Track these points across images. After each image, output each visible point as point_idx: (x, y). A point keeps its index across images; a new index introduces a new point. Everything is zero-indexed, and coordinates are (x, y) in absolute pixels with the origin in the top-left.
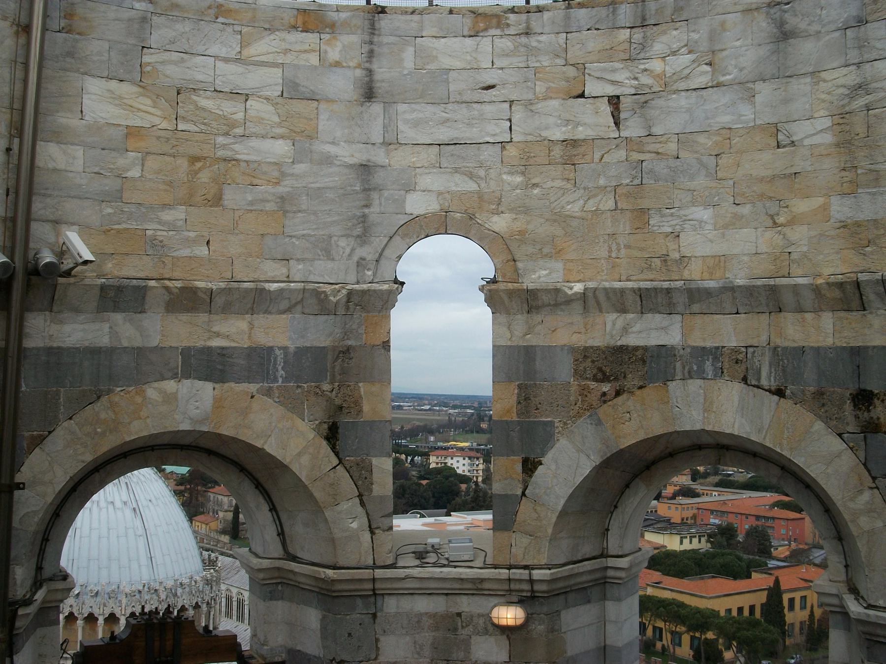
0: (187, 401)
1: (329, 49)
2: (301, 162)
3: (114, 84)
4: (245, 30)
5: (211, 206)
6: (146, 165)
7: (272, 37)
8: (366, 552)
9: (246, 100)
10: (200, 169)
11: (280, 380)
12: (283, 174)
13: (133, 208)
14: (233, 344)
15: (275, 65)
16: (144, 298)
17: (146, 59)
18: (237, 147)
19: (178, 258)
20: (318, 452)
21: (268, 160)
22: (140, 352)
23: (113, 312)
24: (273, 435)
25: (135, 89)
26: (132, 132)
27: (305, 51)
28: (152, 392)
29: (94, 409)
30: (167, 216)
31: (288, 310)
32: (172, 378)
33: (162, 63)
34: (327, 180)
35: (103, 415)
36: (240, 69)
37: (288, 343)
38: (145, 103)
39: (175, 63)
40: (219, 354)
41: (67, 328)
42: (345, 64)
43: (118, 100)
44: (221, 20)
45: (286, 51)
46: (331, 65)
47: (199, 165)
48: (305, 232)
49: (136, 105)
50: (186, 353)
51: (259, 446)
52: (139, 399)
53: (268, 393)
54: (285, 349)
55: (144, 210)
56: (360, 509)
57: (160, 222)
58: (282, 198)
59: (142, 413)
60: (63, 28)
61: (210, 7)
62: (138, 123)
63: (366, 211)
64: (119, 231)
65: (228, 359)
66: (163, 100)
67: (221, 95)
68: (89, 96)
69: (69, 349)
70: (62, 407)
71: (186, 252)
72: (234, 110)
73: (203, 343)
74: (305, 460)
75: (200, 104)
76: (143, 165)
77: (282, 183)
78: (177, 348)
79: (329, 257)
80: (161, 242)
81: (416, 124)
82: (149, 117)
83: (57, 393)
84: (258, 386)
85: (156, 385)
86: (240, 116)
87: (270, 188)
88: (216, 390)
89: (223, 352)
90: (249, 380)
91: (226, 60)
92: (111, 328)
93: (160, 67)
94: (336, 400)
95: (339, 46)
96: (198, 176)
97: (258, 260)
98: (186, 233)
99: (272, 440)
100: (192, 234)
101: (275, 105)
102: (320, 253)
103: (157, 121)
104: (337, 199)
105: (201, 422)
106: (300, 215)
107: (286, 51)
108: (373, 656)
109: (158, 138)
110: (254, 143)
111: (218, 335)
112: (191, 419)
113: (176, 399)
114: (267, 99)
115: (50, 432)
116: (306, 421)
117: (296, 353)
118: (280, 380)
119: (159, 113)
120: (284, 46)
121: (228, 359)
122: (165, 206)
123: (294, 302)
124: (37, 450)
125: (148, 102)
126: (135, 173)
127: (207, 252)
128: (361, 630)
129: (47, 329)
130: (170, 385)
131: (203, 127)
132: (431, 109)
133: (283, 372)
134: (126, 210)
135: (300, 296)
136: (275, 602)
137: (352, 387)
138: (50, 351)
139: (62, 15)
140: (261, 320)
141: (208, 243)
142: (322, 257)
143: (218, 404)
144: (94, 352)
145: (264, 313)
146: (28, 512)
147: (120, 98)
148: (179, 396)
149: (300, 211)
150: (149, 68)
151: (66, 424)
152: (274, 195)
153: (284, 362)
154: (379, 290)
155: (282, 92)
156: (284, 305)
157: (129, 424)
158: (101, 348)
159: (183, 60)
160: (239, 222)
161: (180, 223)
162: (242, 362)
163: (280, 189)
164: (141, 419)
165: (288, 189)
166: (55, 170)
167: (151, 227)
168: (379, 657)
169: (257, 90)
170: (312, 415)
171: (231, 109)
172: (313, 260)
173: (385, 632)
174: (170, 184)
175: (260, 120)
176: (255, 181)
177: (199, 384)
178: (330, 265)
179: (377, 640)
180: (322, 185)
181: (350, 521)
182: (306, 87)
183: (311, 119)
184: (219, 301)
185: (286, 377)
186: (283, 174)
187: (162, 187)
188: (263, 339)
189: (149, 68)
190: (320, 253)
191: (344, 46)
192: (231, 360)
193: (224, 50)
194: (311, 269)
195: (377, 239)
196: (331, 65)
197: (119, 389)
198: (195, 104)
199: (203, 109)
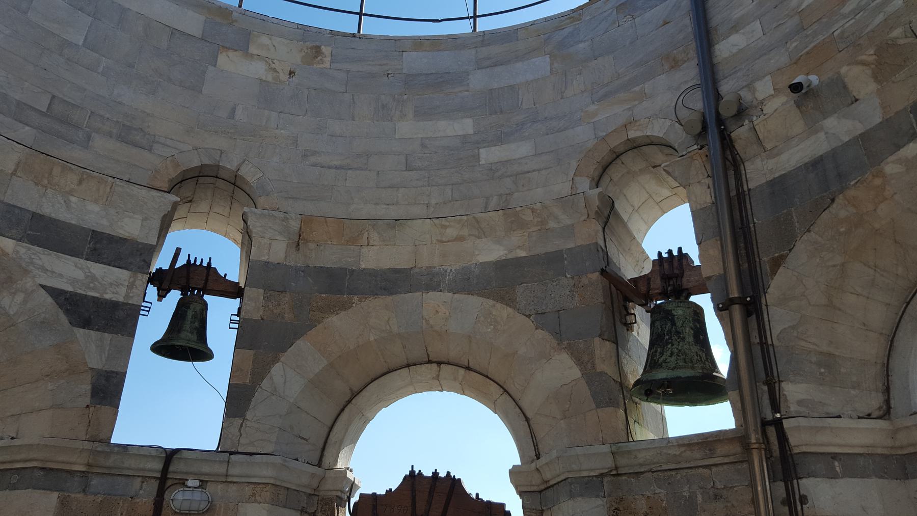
19: (873, 31)
22: (865, 137)
23: (825, 119)
29: (830, 212)
35: (843, 214)
52: (878, 182)
69: (790, 172)
70: (796, 224)
78: (905, 109)
92: (826, 133)
115: (790, 250)
124: (781, 270)
129: (765, 167)
138: (772, 183)
144: (816, 164)
146: (785, 329)
151: (805, 237)
157: (875, 210)
158: (821, 156)
164: (886, 199)
197: (852, 183)
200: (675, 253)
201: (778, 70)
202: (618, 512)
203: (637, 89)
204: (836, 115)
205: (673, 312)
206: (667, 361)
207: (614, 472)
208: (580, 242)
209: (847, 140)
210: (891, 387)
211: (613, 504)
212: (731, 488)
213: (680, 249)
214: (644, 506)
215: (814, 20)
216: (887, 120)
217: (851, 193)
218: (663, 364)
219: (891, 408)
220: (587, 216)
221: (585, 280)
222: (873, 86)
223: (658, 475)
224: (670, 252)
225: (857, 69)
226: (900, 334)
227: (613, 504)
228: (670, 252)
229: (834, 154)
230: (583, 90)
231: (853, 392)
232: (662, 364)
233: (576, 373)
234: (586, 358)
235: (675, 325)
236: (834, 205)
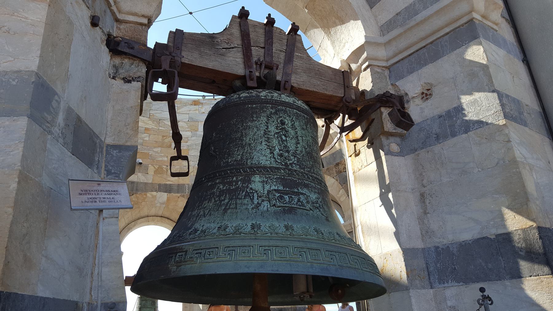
0: (159, 198)
1: (201, 109)
2: (193, 137)
4: (178, 105)
6: (150, 137)
7: (186, 107)
10: (165, 139)
11: (187, 193)
12: (188, 140)
13: (146, 147)
14: (173, 183)
15: (187, 114)
16: (148, 169)
17: (151, 112)
19: (158, 160)
22: (146, 184)
25: (148, 119)
27: (195, 110)
28: (149, 194)
30: (155, 150)
32: (155, 191)
35: (134, 199)
37: (189, 183)
38: (150, 122)
45: (190, 111)
47: (165, 138)
50: (160, 185)
52: (145, 196)
54: (188, 184)
55: (149, 148)
57: (153, 151)
58: (188, 146)
64: (141, 152)
71: (160, 159)
78: (157, 183)
82: (151, 126)
84: (180, 194)
87: (185, 144)
88: (168, 196)
90: (178, 193)
93: (155, 114)
100: (162, 155)
101: (187, 123)
103: (154, 127)
107: (190, 111)
111: (169, 181)
112: (160, 203)
113: (156, 197)
118: (187, 193)
119: (154, 125)
120: (189, 109)
122: (155, 147)
125: (151, 122)
126: (147, 139)
127: (166, 159)
130: (154, 193)
141: (167, 157)
143: (168, 199)
148: (157, 196)
149: (193, 149)
150: (152, 114)
157: (142, 202)
159: (161, 113)
161: (159, 152)
167: (151, 153)
174: (156, 142)
183: (197, 126)
186: (188, 140)
189: (152, 114)
199: (167, 125)
204: (142, 174)
209: (142, 182)
215: (146, 145)
217: (138, 195)
222: (153, 173)
225: (152, 167)
226: (123, 231)
229: (137, 183)
236: (133, 196)
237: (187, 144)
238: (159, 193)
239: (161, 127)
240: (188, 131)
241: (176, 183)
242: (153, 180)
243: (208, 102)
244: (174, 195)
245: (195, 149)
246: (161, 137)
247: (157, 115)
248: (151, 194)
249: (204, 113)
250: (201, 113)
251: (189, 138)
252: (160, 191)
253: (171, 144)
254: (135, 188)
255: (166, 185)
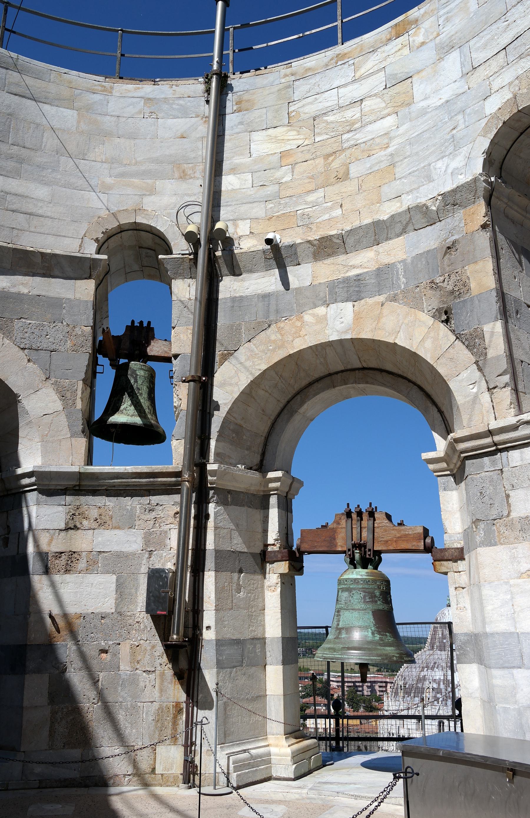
0: (334, 319)
3: (271, 131)
5: (342, 182)
7: (376, 54)
8: (488, 412)
9: (361, 103)
10: (332, 161)
13: (287, 200)
16: (296, 254)
18: (357, 137)
20: (438, 334)
21: (380, 134)
24: (401, 331)
25: (285, 129)
26: (283, 155)
28: (308, 317)
30: (311, 198)
31: (404, 231)
32: (322, 305)
33: (303, 106)
34: (423, 126)
35: (273, 337)
36: (356, 86)
39: (311, 103)
40: (355, 280)
41: (246, 284)
42: (427, 41)
43: (276, 140)
44: (340, 63)
46: (418, 48)
47: (331, 159)
48: (410, 171)
49: (286, 138)
51: (392, 341)
52: (299, 324)
53: (394, 299)
54: (404, 261)
56: (478, 374)
57: (306, 203)
59: (301, 333)
60: (235, 111)
61: (332, 59)
62: (288, 147)
63: (454, 132)
64: (278, 217)
65: (362, 282)
66: (304, 128)
67: (343, 109)
68: (255, 143)
69: (247, 296)
70: (243, 334)
72: (353, 114)
73: (343, 275)
74: (428, 344)
75: (329, 121)
76: (293, 172)
77: (390, 145)
79: (430, 179)
80: (308, 215)
81: (485, 46)
83: (240, 325)
84: (385, 296)
85: (311, 312)
86: (358, 115)
87: (383, 153)
88: (355, 307)
89: (358, 278)
91: (345, 85)
93: (300, 110)
94: (448, 287)
95: (422, 30)
96: (331, 166)
97: (378, 205)
98: (325, 205)
99: (401, 334)
100: (329, 204)
102: (423, 180)
103: (300, 142)
104: (432, 136)
105: (346, 332)
106: (406, 160)
108: (505, 513)
109: (302, 152)
110: (369, 128)
111: (354, 267)
113: (326, 320)
114: (375, 95)
116: (426, 312)
117: (412, 262)
118: (403, 287)
120: (384, 55)
121: (362, 282)
123: (404, 223)
124: (226, 363)
125: (295, 133)
128: (491, 488)
129: (232, 286)
130: (321, 310)
131: (332, 134)
132: (494, 27)
133: (404, 279)
134: (283, 202)
135: (408, 216)
136: (449, 493)
137: (460, 272)
139: (234, 103)
140: (385, 246)
141: (341, 206)
142: (425, 183)
143: (357, 317)
145: (386, 240)
147: (276, 137)
148: (328, 316)
149: (405, 158)
151: (246, 345)
152: (386, 155)
153: (405, 272)
154: (465, 183)
155: (386, 85)
156: (398, 228)
160: (362, 184)
162: (373, 281)
163: (390, 150)
164: (300, 336)
165: (395, 147)
166: (233, 190)
168: (511, 514)
169: (368, 94)
170: (430, 306)
171: (353, 113)
172: (419, 188)
173: (513, 486)
175: (372, 111)
176: (373, 152)
177: (341, 305)
178: (431, 185)
179: (508, 496)
180: (420, 132)
181: (471, 386)
182: (402, 73)
184: (350, 241)
185: (407, 283)
187: (307, 181)
188: (386, 260)
189: (293, 114)
190: (423, 180)
191: (425, 30)
192: (365, 282)
193: (343, 80)
194: (418, 195)
195: (465, 148)
196: (418, 48)
197: (284, 319)
198: (326, 122)
199: (332, 122)
200: (145, 324)
201: (256, 219)
202: (74, 517)
203: (150, 181)
205: (137, 372)
206: (128, 409)
207: (77, 488)
208: (78, 296)
210: (266, 452)
211: (71, 511)
212: (161, 505)
213: (149, 323)
214: (96, 514)
216: (313, 285)
217: (282, 325)
218: (124, 411)
219: (263, 465)
220: (89, 276)
221: (78, 331)
223: (110, 492)
224: (141, 323)
226: (279, 420)
227: (71, 511)
228: (141, 323)
230: (104, 160)
231: (246, 452)
232: (123, 410)
233: (58, 405)
234: (68, 395)
235: (137, 383)
237: (390, 150)
238: (331, 305)
239: (319, 134)
240: (389, 115)
241: (373, 267)
242: (314, 277)
243: (431, 8)
244: (370, 301)
245: (409, 156)
246: (320, 161)
247: (307, 109)
248: (313, 315)
249: (423, 44)
250: (415, 48)
251: (392, 134)
252: (336, 301)
253: (348, 169)
254: (273, 308)
255: (346, 280)
